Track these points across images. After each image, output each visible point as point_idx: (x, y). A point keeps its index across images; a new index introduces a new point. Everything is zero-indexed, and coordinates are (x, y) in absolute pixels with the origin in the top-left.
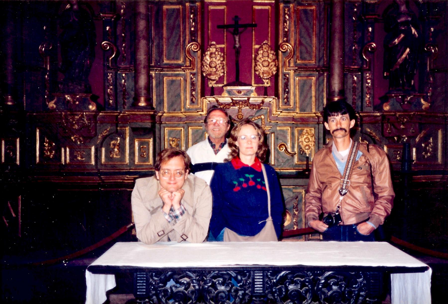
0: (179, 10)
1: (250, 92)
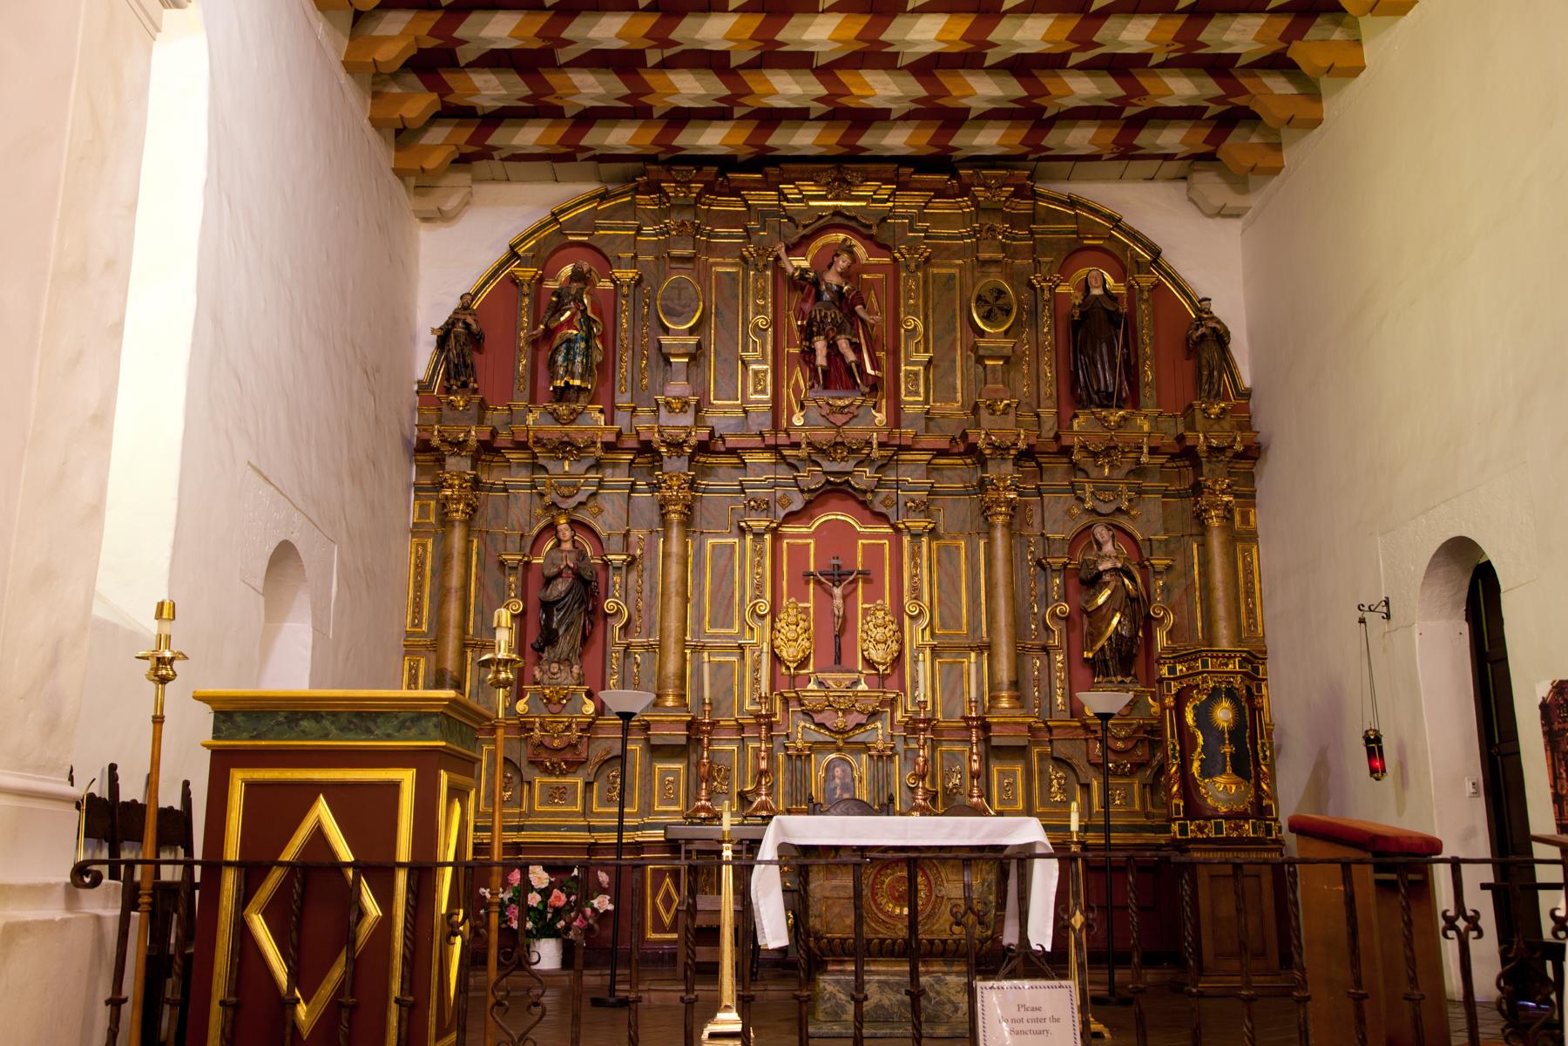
0: (732, 546)
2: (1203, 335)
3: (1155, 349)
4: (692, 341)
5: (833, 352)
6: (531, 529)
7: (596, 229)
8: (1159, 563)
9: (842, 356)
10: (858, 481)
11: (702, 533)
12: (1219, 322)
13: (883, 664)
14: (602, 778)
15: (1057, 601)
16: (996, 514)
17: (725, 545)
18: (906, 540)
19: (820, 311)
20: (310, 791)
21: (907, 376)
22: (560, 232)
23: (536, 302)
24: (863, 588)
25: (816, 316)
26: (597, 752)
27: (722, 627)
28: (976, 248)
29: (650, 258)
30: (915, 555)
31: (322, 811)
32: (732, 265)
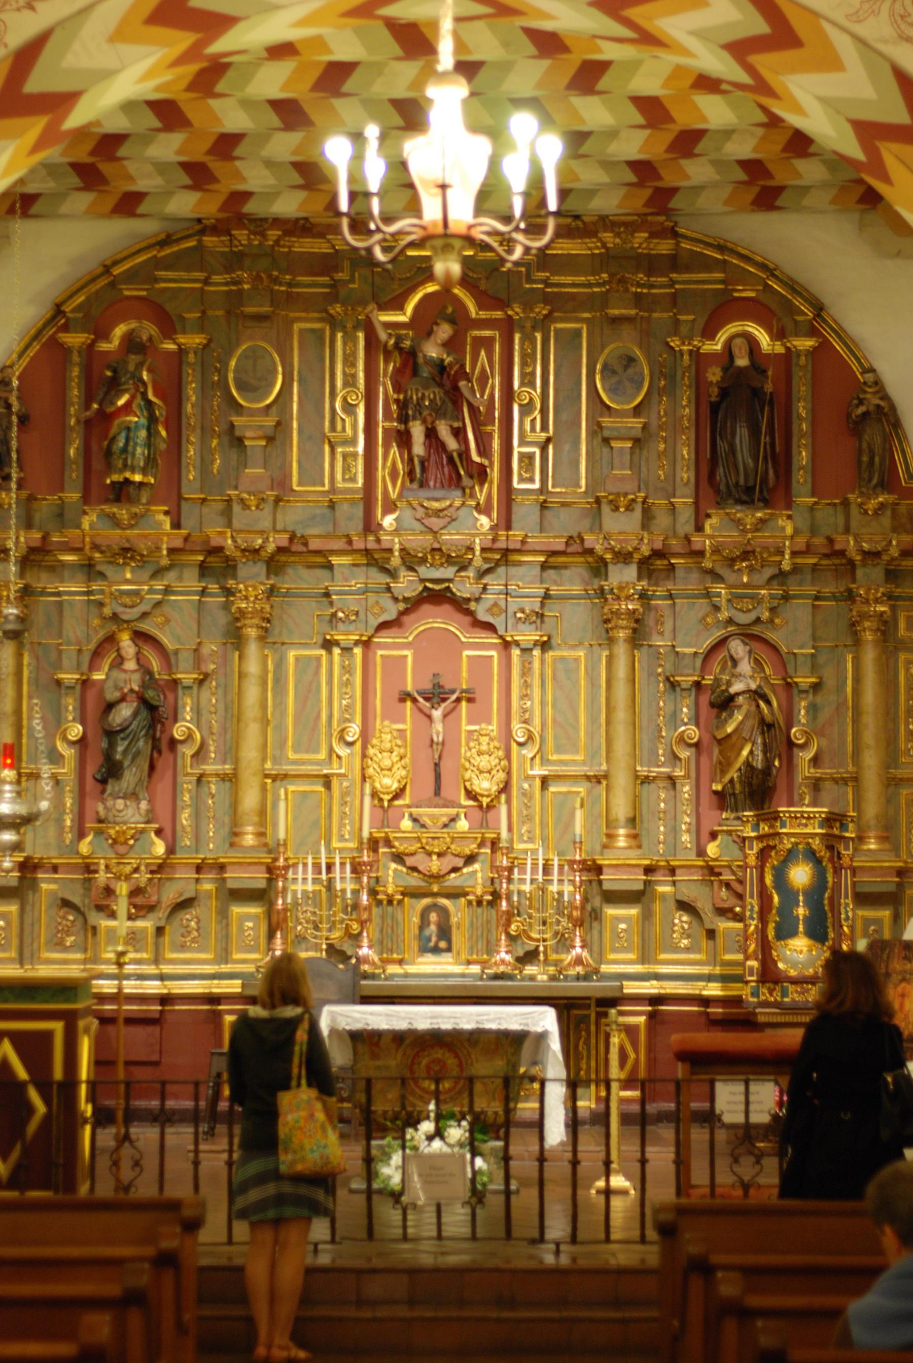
0: (318, 659)
2: (865, 415)
3: (814, 423)
6: (89, 641)
7: (157, 280)
8: (804, 681)
9: (442, 446)
10: (460, 587)
11: (283, 644)
12: (885, 397)
13: (488, 796)
14: (176, 923)
15: (686, 724)
16: (616, 627)
17: (309, 658)
18: (516, 652)
19: (417, 390)
21: (521, 460)
22: (112, 285)
24: (467, 708)
25: (411, 397)
26: (170, 894)
27: (307, 752)
28: (604, 301)
30: (526, 671)
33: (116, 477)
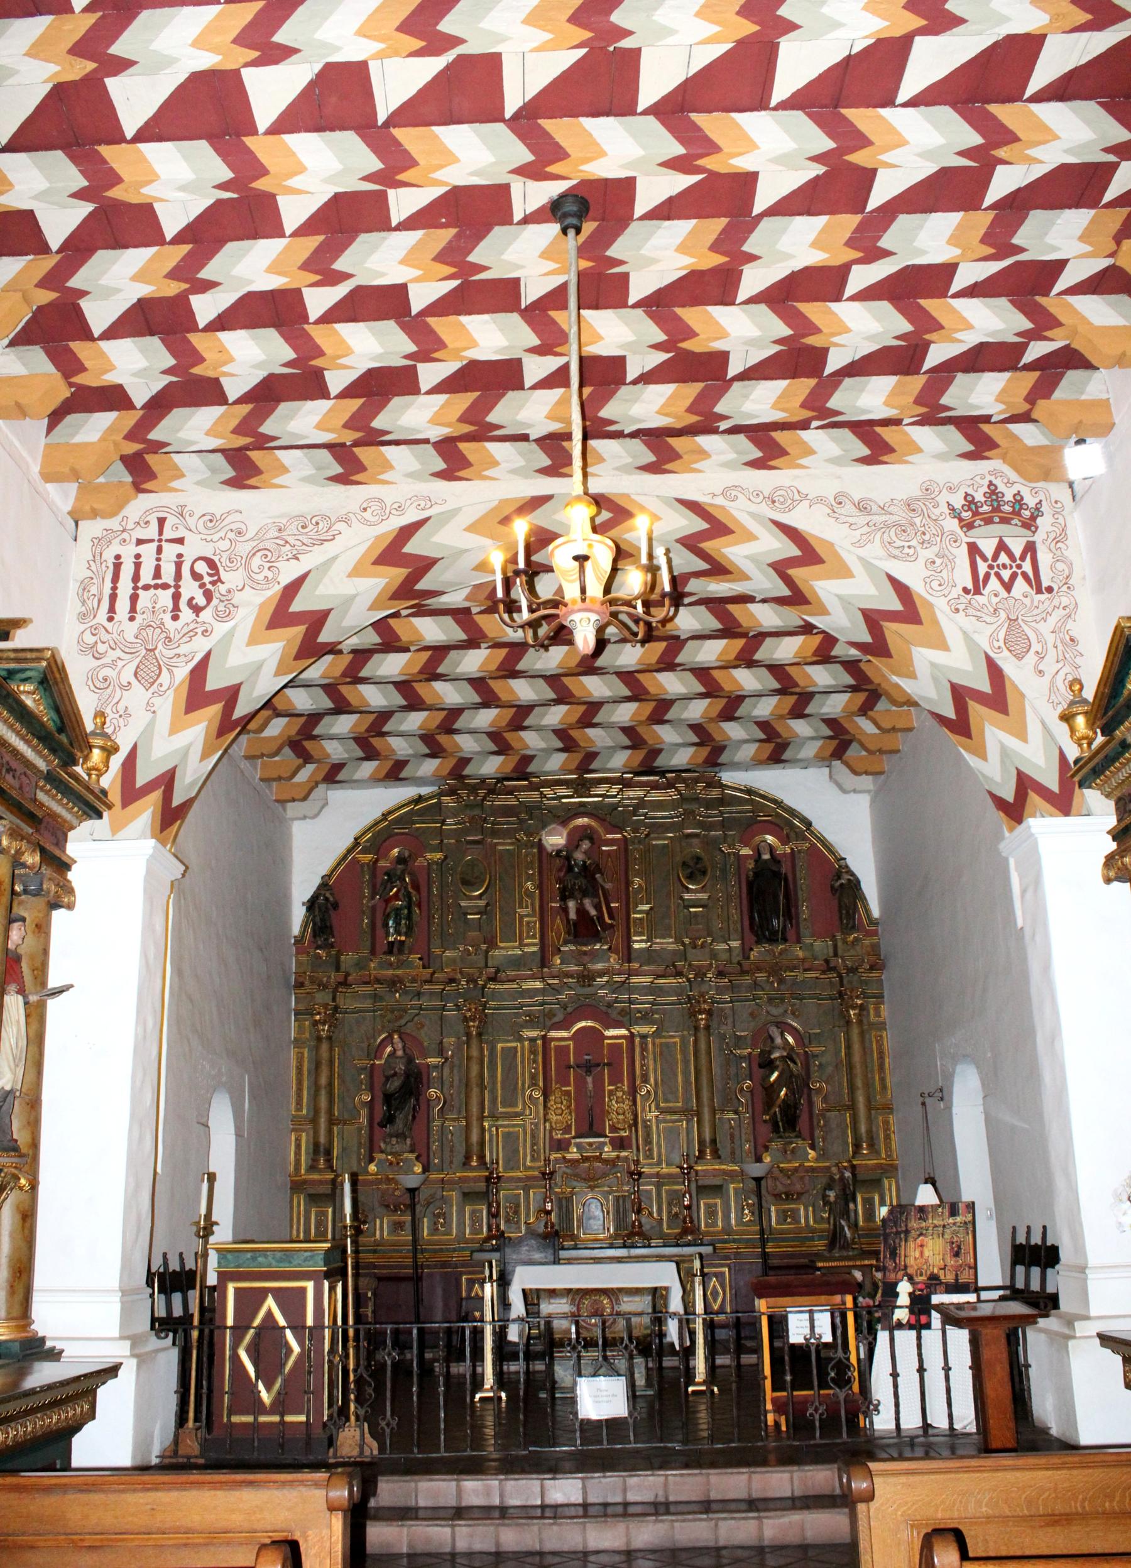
0: (516, 1048)
1: (604, 1144)
4: (482, 903)
5: (581, 911)
6: (375, 1040)
9: (587, 912)
12: (853, 874)
17: (510, 1048)
18: (637, 1040)
20: (264, 1292)
23: (373, 875)
29: (453, 841)
31: (270, 1303)
32: (511, 844)
33: (391, 939)
